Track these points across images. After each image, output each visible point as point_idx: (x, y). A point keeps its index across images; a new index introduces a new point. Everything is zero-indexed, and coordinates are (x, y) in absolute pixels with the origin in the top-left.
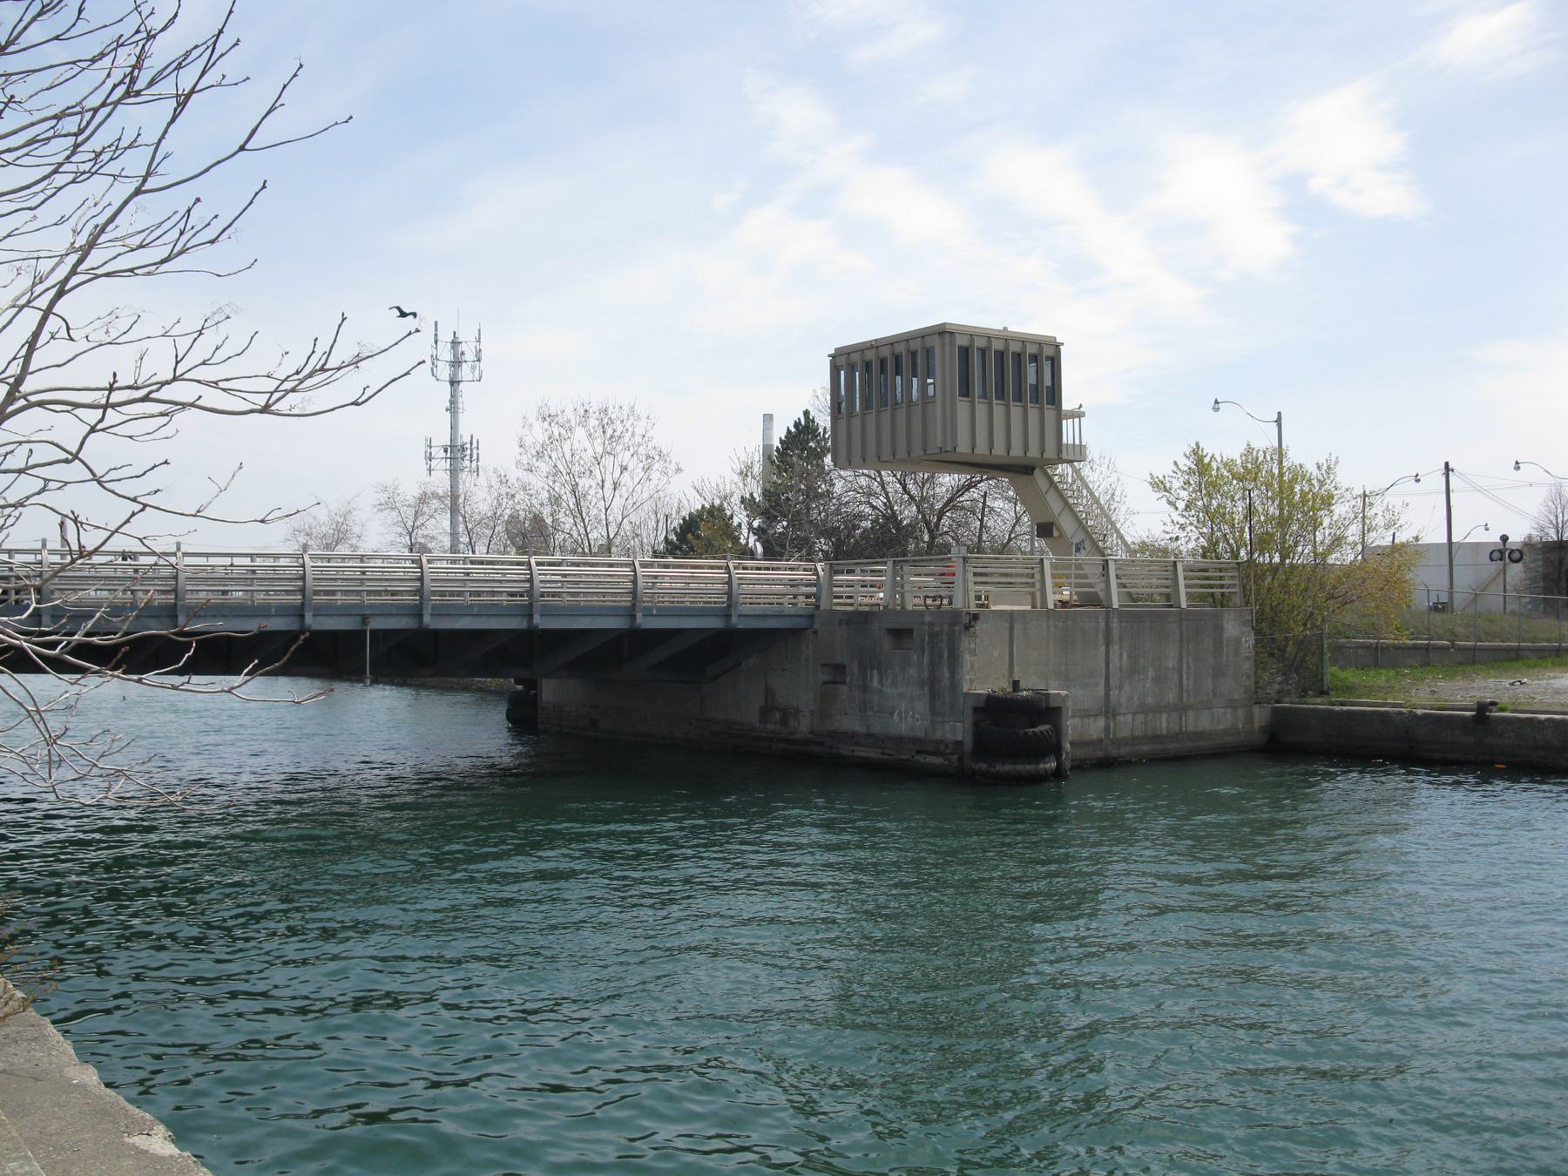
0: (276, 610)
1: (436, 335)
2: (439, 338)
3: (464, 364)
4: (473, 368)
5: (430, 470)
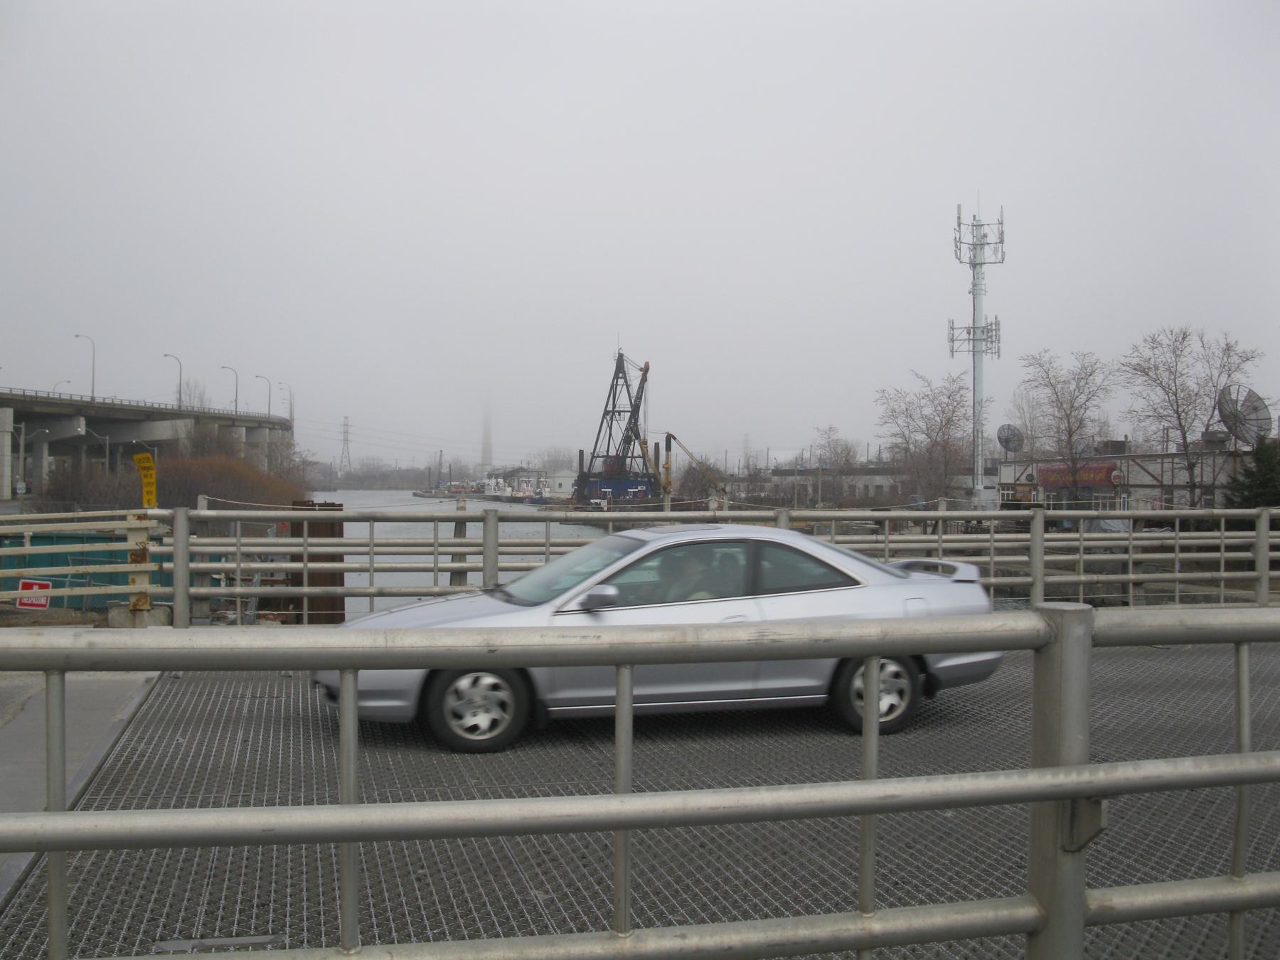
0: (829, 527)
1: (959, 218)
2: (963, 221)
3: (986, 247)
4: (996, 251)
5: (952, 351)
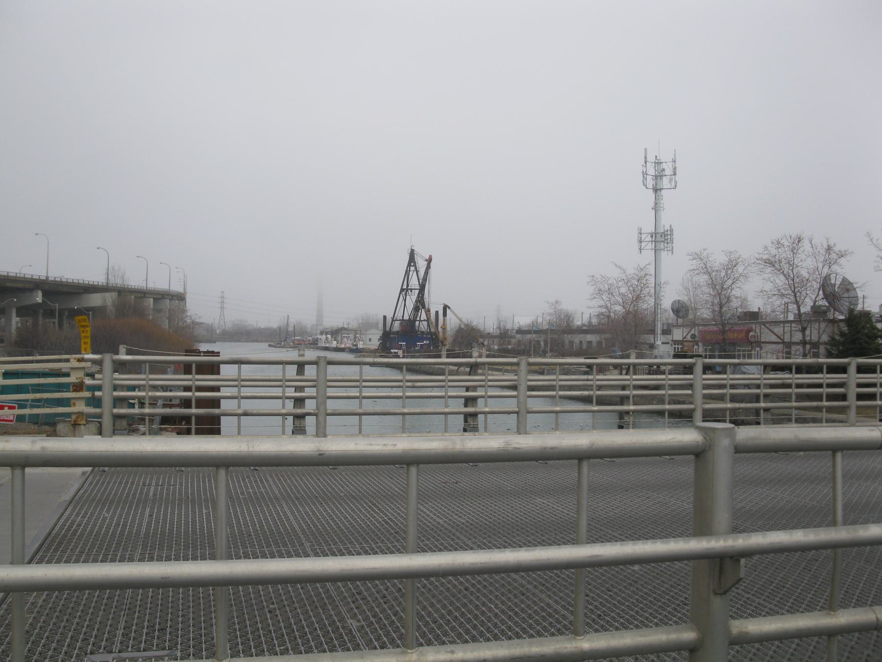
0: (555, 369)
1: (646, 158)
2: (648, 160)
3: (664, 178)
4: (671, 180)
5: (640, 249)
